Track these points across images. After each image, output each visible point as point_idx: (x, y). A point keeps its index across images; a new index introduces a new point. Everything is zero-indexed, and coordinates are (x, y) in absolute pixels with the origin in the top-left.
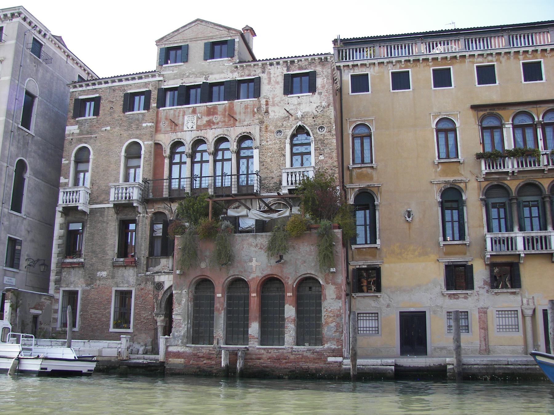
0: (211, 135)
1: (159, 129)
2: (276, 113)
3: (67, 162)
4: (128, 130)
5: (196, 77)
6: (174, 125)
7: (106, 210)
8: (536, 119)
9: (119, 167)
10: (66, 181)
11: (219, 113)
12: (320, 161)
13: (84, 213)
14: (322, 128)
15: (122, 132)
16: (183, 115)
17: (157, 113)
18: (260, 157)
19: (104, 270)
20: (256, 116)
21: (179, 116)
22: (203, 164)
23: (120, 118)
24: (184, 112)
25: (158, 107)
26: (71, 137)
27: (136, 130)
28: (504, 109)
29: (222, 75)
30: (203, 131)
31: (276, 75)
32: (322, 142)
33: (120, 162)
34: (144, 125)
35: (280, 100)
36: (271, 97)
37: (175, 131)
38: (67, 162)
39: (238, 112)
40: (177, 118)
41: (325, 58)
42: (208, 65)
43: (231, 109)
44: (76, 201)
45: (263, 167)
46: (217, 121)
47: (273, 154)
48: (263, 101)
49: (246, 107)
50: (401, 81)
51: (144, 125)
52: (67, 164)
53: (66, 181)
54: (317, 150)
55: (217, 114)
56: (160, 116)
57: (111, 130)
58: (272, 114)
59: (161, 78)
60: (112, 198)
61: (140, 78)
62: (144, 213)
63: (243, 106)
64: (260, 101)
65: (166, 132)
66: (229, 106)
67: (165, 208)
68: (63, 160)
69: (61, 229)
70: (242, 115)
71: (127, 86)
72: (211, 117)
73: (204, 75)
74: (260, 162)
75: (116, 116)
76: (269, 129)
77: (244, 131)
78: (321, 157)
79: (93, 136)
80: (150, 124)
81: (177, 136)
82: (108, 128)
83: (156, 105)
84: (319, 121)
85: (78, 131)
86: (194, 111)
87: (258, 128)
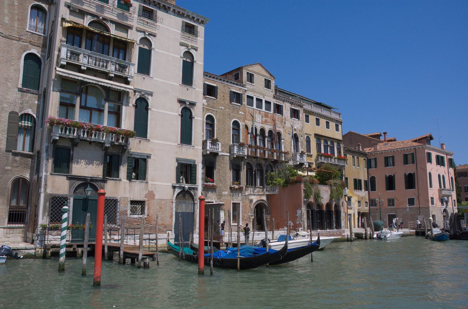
2: (288, 125)
19: (226, 191)
29: (270, 98)
34: (240, 112)
48: (284, 117)
51: (240, 112)
58: (287, 125)
59: (246, 89)
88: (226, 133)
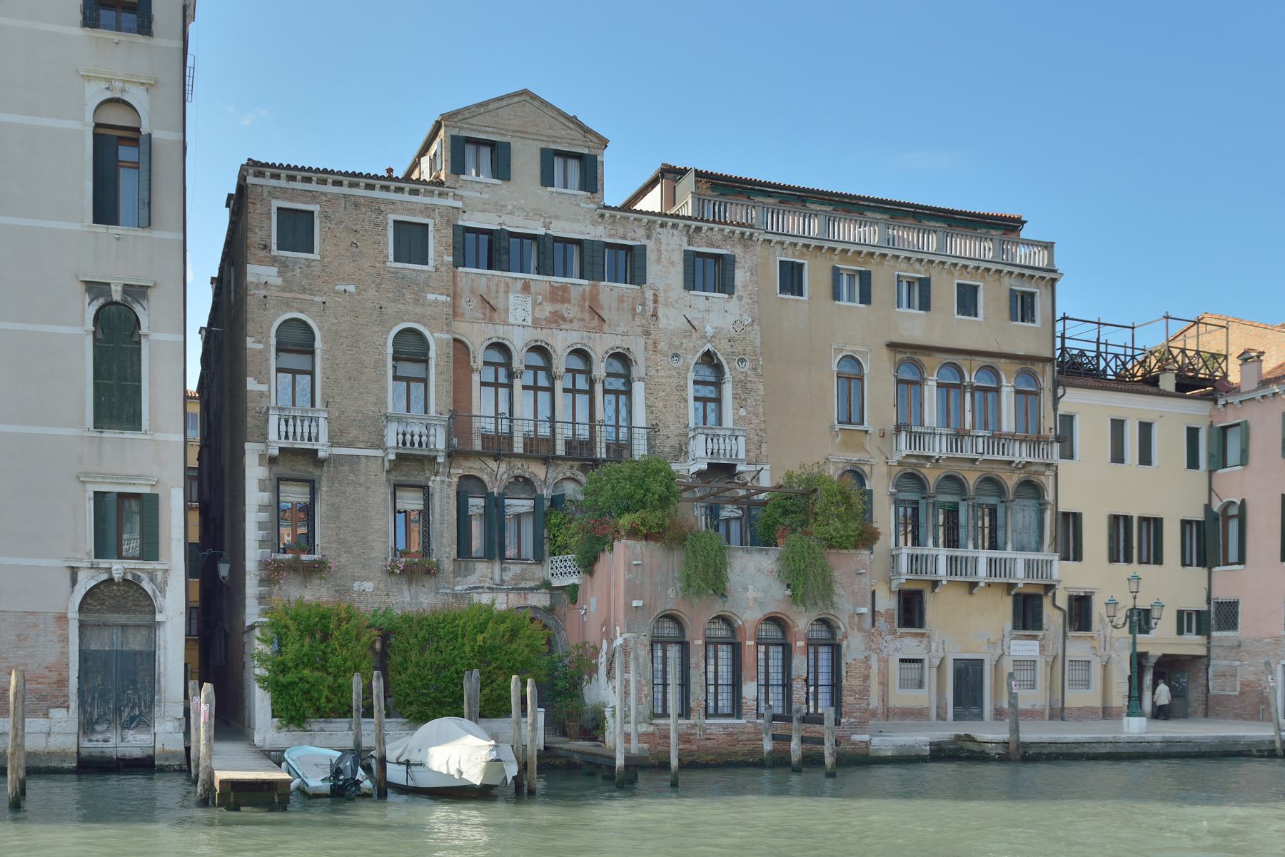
1: (459, 311)
2: (670, 319)
3: (260, 346)
4: (395, 301)
5: (527, 217)
6: (490, 308)
7: (363, 460)
8: (967, 379)
10: (264, 388)
13: (320, 463)
14: (742, 360)
15: (384, 305)
16: (507, 292)
17: (454, 277)
20: (638, 320)
21: (497, 292)
22: (539, 393)
23: (374, 270)
24: (507, 285)
25: (456, 265)
26: (263, 293)
28: (929, 355)
29: (576, 226)
31: (670, 248)
33: (385, 365)
34: (431, 297)
36: (661, 288)
37: (491, 321)
38: (260, 346)
43: (594, 297)
44: (310, 439)
45: (652, 416)
46: (571, 316)
48: (649, 295)
49: (621, 300)
50: (791, 278)
51: (431, 297)
52: (260, 351)
53: (264, 388)
55: (569, 302)
56: (459, 284)
57: (359, 294)
58: (663, 321)
59: (459, 204)
62: (443, 474)
64: (643, 293)
65: (475, 321)
66: (591, 292)
67: (481, 470)
68: (249, 340)
69: (261, 490)
71: (385, 202)
72: (558, 307)
74: (648, 407)
76: (659, 347)
78: (743, 412)
79: (316, 299)
80: (443, 298)
82: (351, 288)
83: (451, 259)
85: (279, 281)
86: (526, 288)
87: (641, 341)
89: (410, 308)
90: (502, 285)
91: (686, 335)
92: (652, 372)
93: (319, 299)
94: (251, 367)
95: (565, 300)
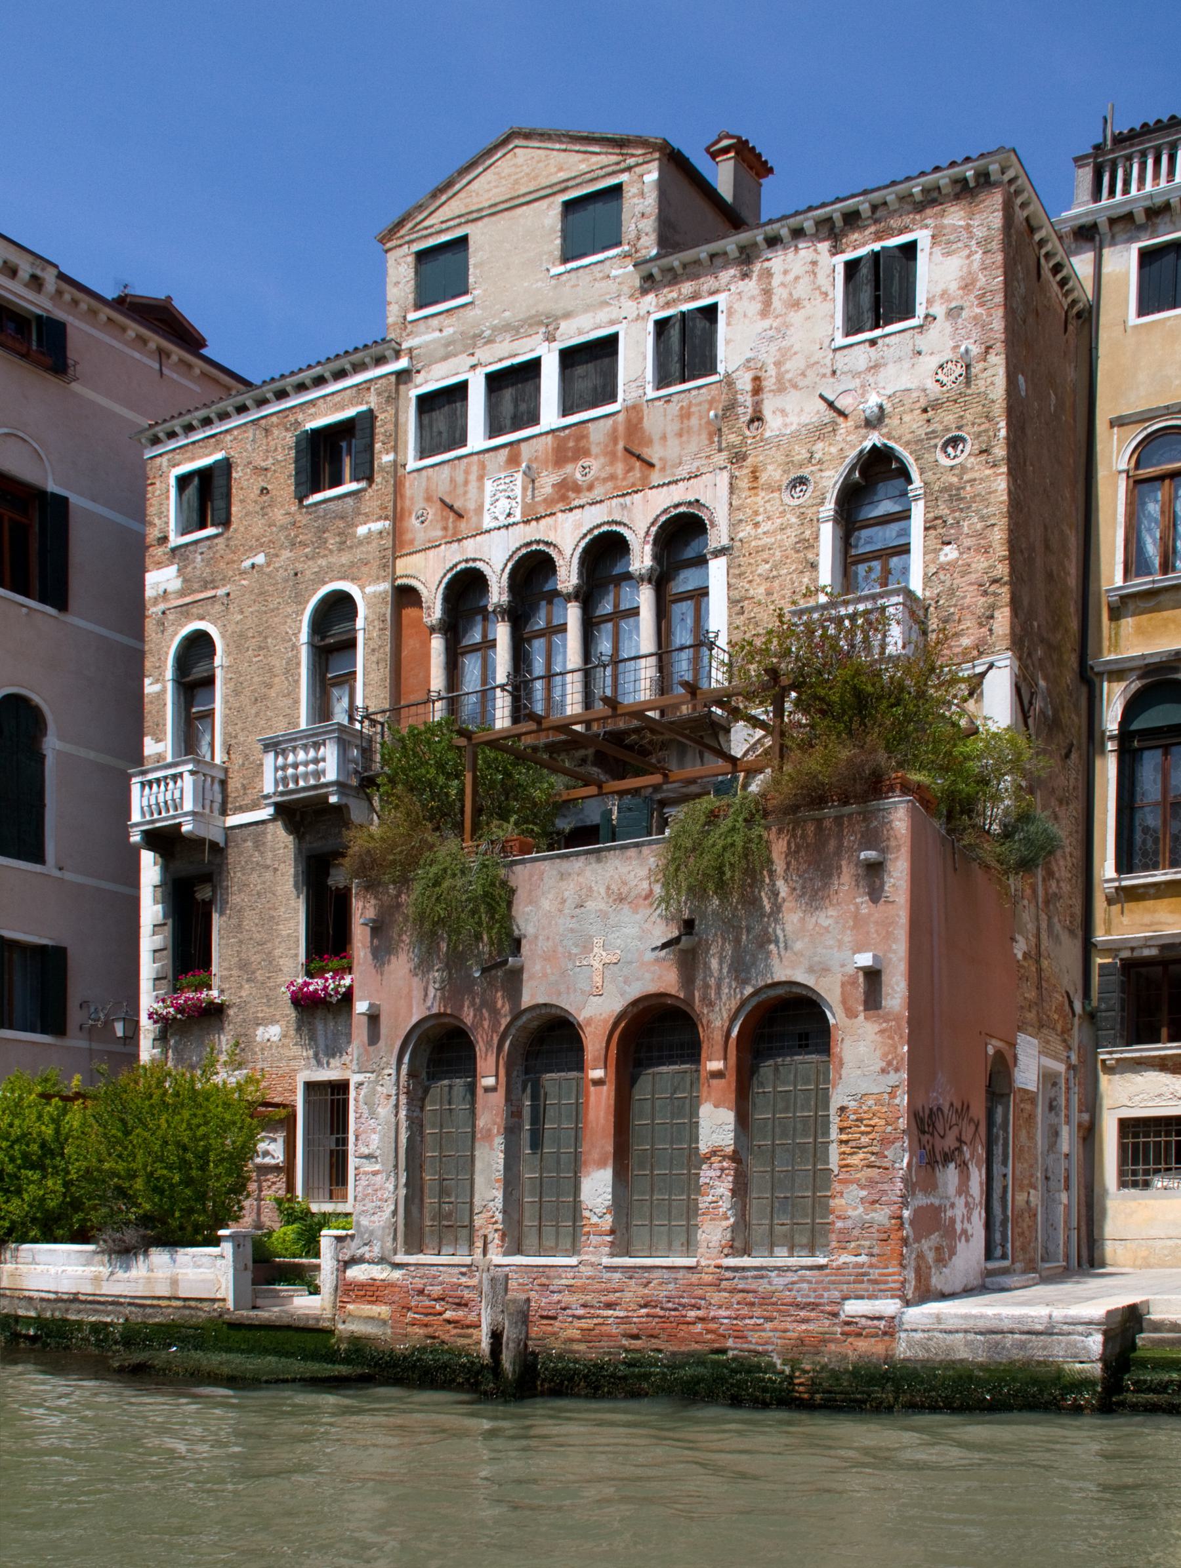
0: (567, 536)
2: (790, 414)
9: (297, 682)
11: (595, 450)
12: (942, 568)
14: (955, 441)
15: (299, 567)
16: (481, 478)
18: (729, 585)
21: (466, 483)
24: (483, 466)
27: (340, 550)
29: (603, 315)
30: (543, 522)
32: (954, 495)
33: (298, 664)
34: (362, 530)
35: (802, 365)
39: (656, 437)
40: (460, 491)
41: (978, 175)
42: (555, 287)
47: (775, 567)
49: (685, 414)
51: (362, 530)
54: (934, 528)
55: (586, 453)
58: (773, 424)
60: (269, 787)
61: (340, 374)
63: (674, 408)
66: (628, 420)
70: (673, 442)
73: (540, 323)
75: (278, 515)
76: (763, 478)
77: (676, 501)
81: (464, 551)
84: (947, 419)
87: (724, 477)
88: (272, 693)
89: (332, 559)
90: (475, 468)
91: (823, 432)
92: (745, 531)
93: (221, 592)
94: (149, 723)
95: (581, 452)
